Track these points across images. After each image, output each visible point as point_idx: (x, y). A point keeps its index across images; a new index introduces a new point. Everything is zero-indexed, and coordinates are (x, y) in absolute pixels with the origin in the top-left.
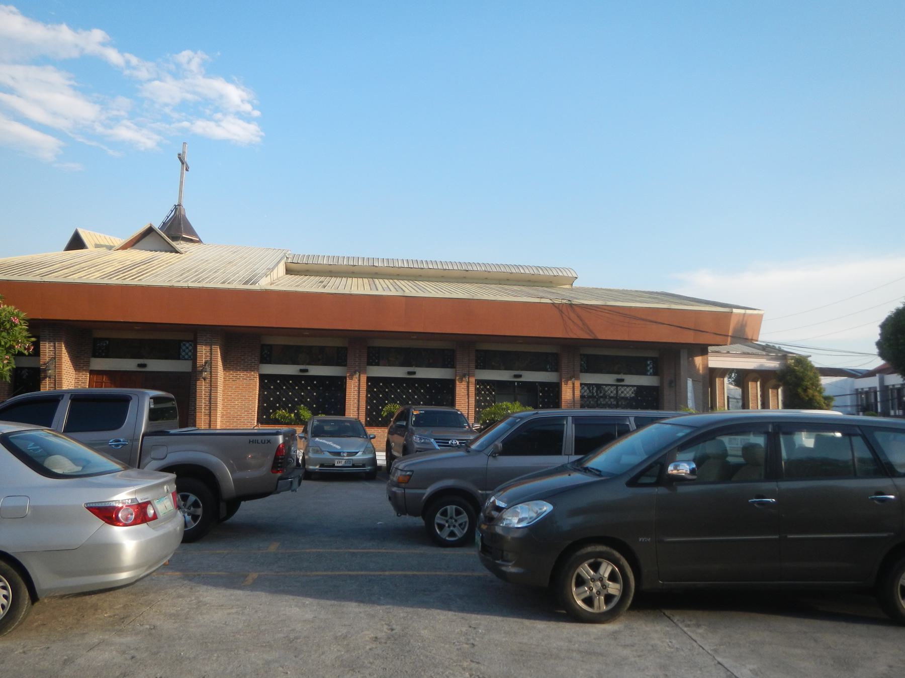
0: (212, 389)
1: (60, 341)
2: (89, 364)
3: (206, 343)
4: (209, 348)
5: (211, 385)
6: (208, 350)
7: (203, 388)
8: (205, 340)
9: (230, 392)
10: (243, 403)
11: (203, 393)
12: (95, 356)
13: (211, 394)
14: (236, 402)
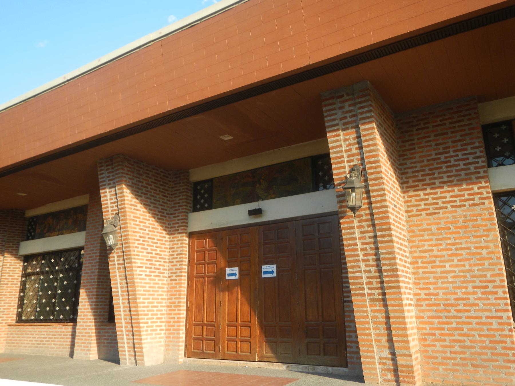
0: (378, 234)
1: (120, 182)
2: (187, 223)
3: (344, 124)
5: (374, 225)
7: (357, 234)
8: (341, 119)
9: (426, 243)
10: (467, 267)
11: (359, 246)
12: (195, 210)
13: (377, 248)
14: (447, 265)
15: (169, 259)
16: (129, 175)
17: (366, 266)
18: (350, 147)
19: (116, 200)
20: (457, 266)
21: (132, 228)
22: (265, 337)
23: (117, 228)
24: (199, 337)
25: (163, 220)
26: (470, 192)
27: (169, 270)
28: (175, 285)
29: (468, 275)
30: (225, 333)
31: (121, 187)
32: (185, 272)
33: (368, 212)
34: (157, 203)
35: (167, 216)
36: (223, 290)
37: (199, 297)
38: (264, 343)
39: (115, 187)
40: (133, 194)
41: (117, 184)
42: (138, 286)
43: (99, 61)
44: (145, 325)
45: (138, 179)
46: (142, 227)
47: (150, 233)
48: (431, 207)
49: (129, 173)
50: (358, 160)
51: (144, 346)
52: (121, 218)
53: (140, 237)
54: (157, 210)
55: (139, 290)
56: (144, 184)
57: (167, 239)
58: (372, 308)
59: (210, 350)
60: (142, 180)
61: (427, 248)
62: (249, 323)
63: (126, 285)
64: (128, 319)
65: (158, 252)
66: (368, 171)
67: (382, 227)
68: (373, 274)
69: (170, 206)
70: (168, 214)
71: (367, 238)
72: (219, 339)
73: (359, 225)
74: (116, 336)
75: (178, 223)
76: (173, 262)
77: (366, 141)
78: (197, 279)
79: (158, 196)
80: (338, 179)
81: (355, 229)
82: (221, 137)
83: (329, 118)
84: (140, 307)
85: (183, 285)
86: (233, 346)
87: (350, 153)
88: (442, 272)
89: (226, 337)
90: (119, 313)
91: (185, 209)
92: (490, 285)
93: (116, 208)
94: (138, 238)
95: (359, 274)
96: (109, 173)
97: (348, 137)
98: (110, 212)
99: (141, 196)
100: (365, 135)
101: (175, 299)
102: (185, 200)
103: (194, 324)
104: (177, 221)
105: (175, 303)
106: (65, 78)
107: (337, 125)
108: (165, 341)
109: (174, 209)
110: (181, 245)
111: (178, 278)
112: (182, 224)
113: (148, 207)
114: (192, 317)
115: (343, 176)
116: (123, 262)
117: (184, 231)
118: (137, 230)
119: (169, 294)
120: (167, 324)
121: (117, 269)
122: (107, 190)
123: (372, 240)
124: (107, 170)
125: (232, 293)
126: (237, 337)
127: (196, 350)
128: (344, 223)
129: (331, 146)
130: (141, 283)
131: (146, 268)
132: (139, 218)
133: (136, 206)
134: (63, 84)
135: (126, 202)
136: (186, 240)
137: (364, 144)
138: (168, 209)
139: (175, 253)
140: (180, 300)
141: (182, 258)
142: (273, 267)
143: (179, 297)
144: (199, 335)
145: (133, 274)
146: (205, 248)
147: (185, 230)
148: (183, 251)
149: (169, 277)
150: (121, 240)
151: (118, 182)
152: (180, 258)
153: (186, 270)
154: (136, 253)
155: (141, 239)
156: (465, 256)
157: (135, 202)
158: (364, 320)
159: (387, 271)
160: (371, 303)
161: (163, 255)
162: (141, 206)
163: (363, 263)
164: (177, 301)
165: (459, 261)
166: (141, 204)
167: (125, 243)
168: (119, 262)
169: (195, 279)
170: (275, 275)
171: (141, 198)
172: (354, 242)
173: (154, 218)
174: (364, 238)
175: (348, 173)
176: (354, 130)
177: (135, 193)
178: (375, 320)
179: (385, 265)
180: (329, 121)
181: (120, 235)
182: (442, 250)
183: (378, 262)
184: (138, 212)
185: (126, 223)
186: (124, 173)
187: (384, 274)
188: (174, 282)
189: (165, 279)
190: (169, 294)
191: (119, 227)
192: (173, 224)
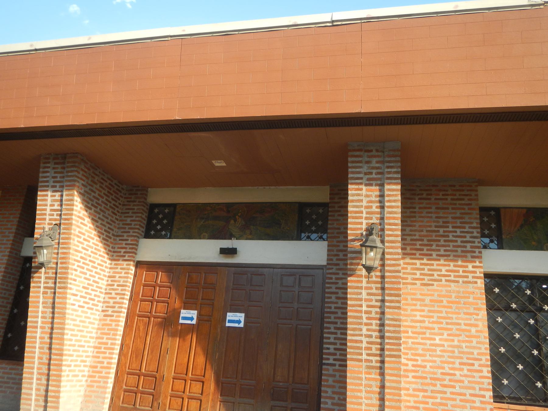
0: (387, 298)
1: (71, 187)
2: (136, 250)
3: (368, 179)
4: (378, 193)
5: (383, 289)
6: (374, 199)
7: (364, 295)
8: (366, 174)
9: (418, 313)
10: (456, 343)
12: (147, 236)
13: (383, 313)
14: (437, 338)
15: (106, 290)
16: (84, 180)
17: (368, 330)
18: (370, 204)
19: (59, 208)
20: (446, 340)
21: (75, 245)
22: (221, 395)
23: (53, 243)
24: (132, 388)
25: (107, 240)
26: (465, 269)
27: (104, 302)
28: (110, 323)
29: (456, 350)
30: (169, 387)
31: (71, 192)
32: (125, 308)
33: (379, 274)
34: (106, 220)
35: (113, 237)
36: (173, 335)
37: (139, 340)
38: (219, 402)
39: (62, 191)
40: (83, 204)
41: (66, 188)
42: (68, 319)
43: (89, 39)
44: (68, 369)
45: (91, 188)
46: (85, 246)
47: (92, 255)
48: (426, 278)
49: (84, 178)
50: (377, 218)
51: (61, 395)
52: (62, 231)
53: (82, 258)
54: (104, 228)
55: (68, 324)
56: (96, 195)
57: (107, 265)
58: (367, 376)
59: (144, 406)
60: (94, 190)
61: (418, 318)
62: (202, 377)
63: (51, 315)
64: (44, 358)
65: (96, 279)
66: (387, 232)
67: (392, 292)
68: (373, 340)
69: (117, 226)
70: (113, 235)
71: (374, 301)
72: (160, 393)
73: (367, 286)
74: (21, 379)
75: (125, 248)
76: (111, 294)
77: (389, 201)
78: (139, 318)
79: (107, 212)
80: (352, 235)
81: (362, 289)
82: (213, 162)
83: (354, 170)
84: (66, 345)
85: (120, 323)
86: (177, 403)
87: (369, 210)
88: (431, 345)
89: (170, 392)
90: (34, 350)
91: (138, 233)
92: (476, 363)
93: (58, 217)
94: (79, 259)
95: (360, 337)
96: (55, 173)
97: (370, 193)
98: (47, 221)
99: (90, 209)
100: (389, 196)
101: (107, 339)
102: (139, 223)
103: (128, 372)
104: (124, 246)
105: (106, 344)
106: (31, 46)
107: (361, 178)
108: (86, 391)
109: (123, 230)
110: (126, 275)
111: (115, 314)
112: (130, 250)
113: (96, 224)
114: (126, 363)
115: (359, 232)
116: (53, 285)
117: (132, 259)
118: (80, 249)
119: (99, 332)
120: (91, 370)
121: (41, 293)
122: (49, 193)
123: (379, 304)
124: (54, 168)
125: (184, 340)
126: (184, 392)
127: (125, 404)
128: (352, 281)
129: (350, 199)
130: (72, 315)
131: (81, 297)
132: (84, 234)
133: (84, 220)
134: (28, 53)
135: (74, 212)
136: (132, 270)
137: (387, 204)
138: (115, 229)
139: (116, 284)
140: (114, 342)
141: (125, 290)
142: (241, 316)
143: (113, 337)
144: (133, 387)
145: (66, 302)
146: (155, 282)
147: (134, 257)
148: (127, 282)
149: (103, 311)
150: (57, 258)
151: (67, 186)
152: (122, 290)
153: (127, 306)
154: (73, 277)
155: (82, 261)
156: (454, 332)
157: (84, 215)
158: (357, 388)
159: (389, 338)
160: (366, 370)
161: (100, 283)
162: (89, 220)
163: (365, 327)
164: (110, 341)
165: (448, 335)
166: (89, 217)
167: (61, 263)
168: (46, 285)
169: (137, 317)
170: (242, 325)
171: (90, 211)
172: (359, 303)
173: (99, 237)
174: (371, 300)
175: (365, 231)
176: (378, 187)
177: (86, 203)
178: (369, 389)
179: (389, 331)
180: (353, 173)
181: (56, 251)
182: (433, 322)
183: (382, 327)
184: (85, 228)
185: (69, 238)
186: (78, 177)
187: (387, 341)
188: (109, 318)
189: (98, 313)
190: (99, 332)
191: (57, 241)
192: (118, 248)
